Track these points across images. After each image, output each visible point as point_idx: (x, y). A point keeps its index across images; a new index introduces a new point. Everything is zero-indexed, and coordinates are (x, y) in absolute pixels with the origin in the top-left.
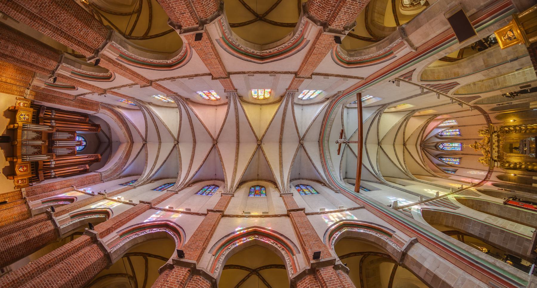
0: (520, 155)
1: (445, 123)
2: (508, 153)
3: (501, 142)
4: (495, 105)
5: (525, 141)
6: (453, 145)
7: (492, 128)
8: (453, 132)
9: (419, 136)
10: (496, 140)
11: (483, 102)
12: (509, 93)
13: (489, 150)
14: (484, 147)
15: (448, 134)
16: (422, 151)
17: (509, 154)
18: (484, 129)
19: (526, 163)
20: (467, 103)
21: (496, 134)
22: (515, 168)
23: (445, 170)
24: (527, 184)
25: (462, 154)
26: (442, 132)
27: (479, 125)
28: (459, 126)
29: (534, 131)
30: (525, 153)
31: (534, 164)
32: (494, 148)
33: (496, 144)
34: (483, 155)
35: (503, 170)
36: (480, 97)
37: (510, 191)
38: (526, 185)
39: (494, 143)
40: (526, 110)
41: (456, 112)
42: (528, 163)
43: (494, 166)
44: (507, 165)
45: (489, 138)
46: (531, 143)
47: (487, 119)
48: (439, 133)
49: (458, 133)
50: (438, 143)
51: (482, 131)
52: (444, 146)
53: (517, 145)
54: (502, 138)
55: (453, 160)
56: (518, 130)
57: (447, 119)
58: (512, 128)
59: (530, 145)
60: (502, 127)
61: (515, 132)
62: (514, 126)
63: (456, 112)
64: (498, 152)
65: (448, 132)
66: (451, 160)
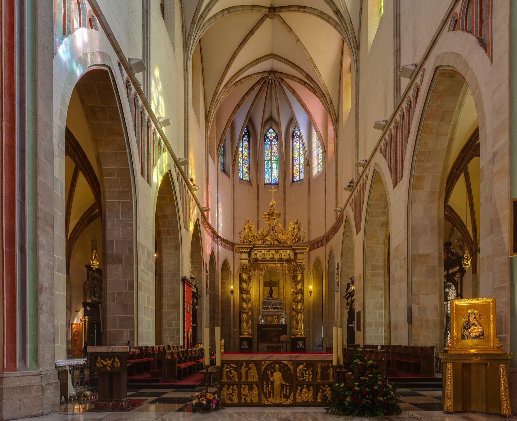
0: (261, 298)
1: (318, 147)
2: (264, 279)
3: (279, 265)
4: (338, 260)
5: (281, 308)
6: (275, 166)
7: (301, 249)
8: (300, 164)
9: (294, 65)
10: (283, 257)
11: (347, 237)
12: (354, 290)
13: (267, 243)
14: (272, 233)
16: (259, 77)
17: (262, 281)
18: (301, 234)
19: (250, 309)
20: (351, 201)
21: (292, 256)
22: (242, 290)
23: (224, 147)
24: (222, 312)
25: (258, 186)
26: (300, 137)
27: (309, 224)
28: (309, 178)
29: (294, 322)
30: (263, 308)
31: (250, 322)
32: (269, 251)
33: (277, 257)
34: (258, 230)
35: (237, 271)
36: (358, 233)
37: (207, 287)
38: (220, 312)
39: (277, 252)
40: (324, 315)
41: (337, 175)
42: (250, 313)
43: (241, 253)
44: (245, 276)
45: (285, 242)
46: (279, 317)
48: (299, 130)
49: (297, 178)
50: (278, 125)
51: (299, 229)
52: (271, 141)
53: (275, 295)
54: (286, 267)
55: (246, 166)
56: (296, 298)
57: (325, 151)
58: (299, 287)
59: (275, 315)
60: (302, 268)
61: (294, 292)
62: (303, 291)
63: (337, 175)
64: (264, 260)
65: (300, 154)
66: (246, 159)
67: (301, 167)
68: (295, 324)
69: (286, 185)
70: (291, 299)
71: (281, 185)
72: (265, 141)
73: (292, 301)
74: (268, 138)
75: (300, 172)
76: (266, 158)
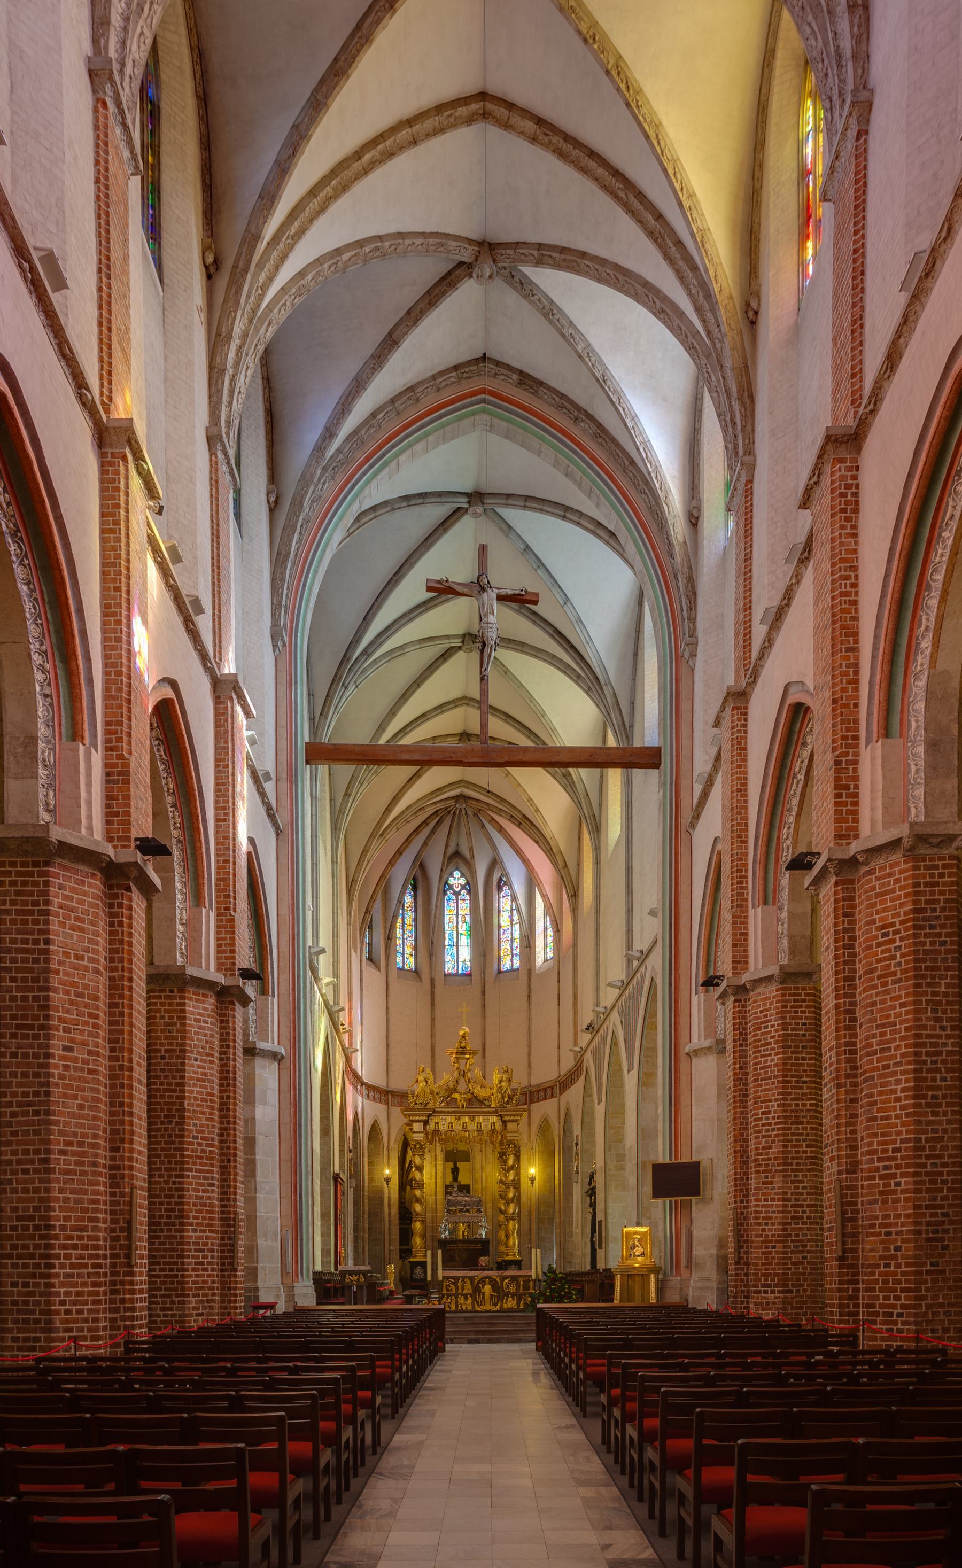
6: (464, 941)
8: (512, 940)
15: (505, 920)
24: (369, 1216)
27: (529, 1055)
35: (395, 1141)
47: (545, 1089)
49: (506, 964)
52: (457, 894)
55: (410, 942)
65: (512, 920)
66: (410, 930)
67: (515, 945)
68: (504, 1238)
69: (487, 979)
70: (497, 1194)
71: (476, 977)
72: (445, 893)
73: (497, 1197)
74: (451, 887)
75: (512, 955)
76: (447, 928)
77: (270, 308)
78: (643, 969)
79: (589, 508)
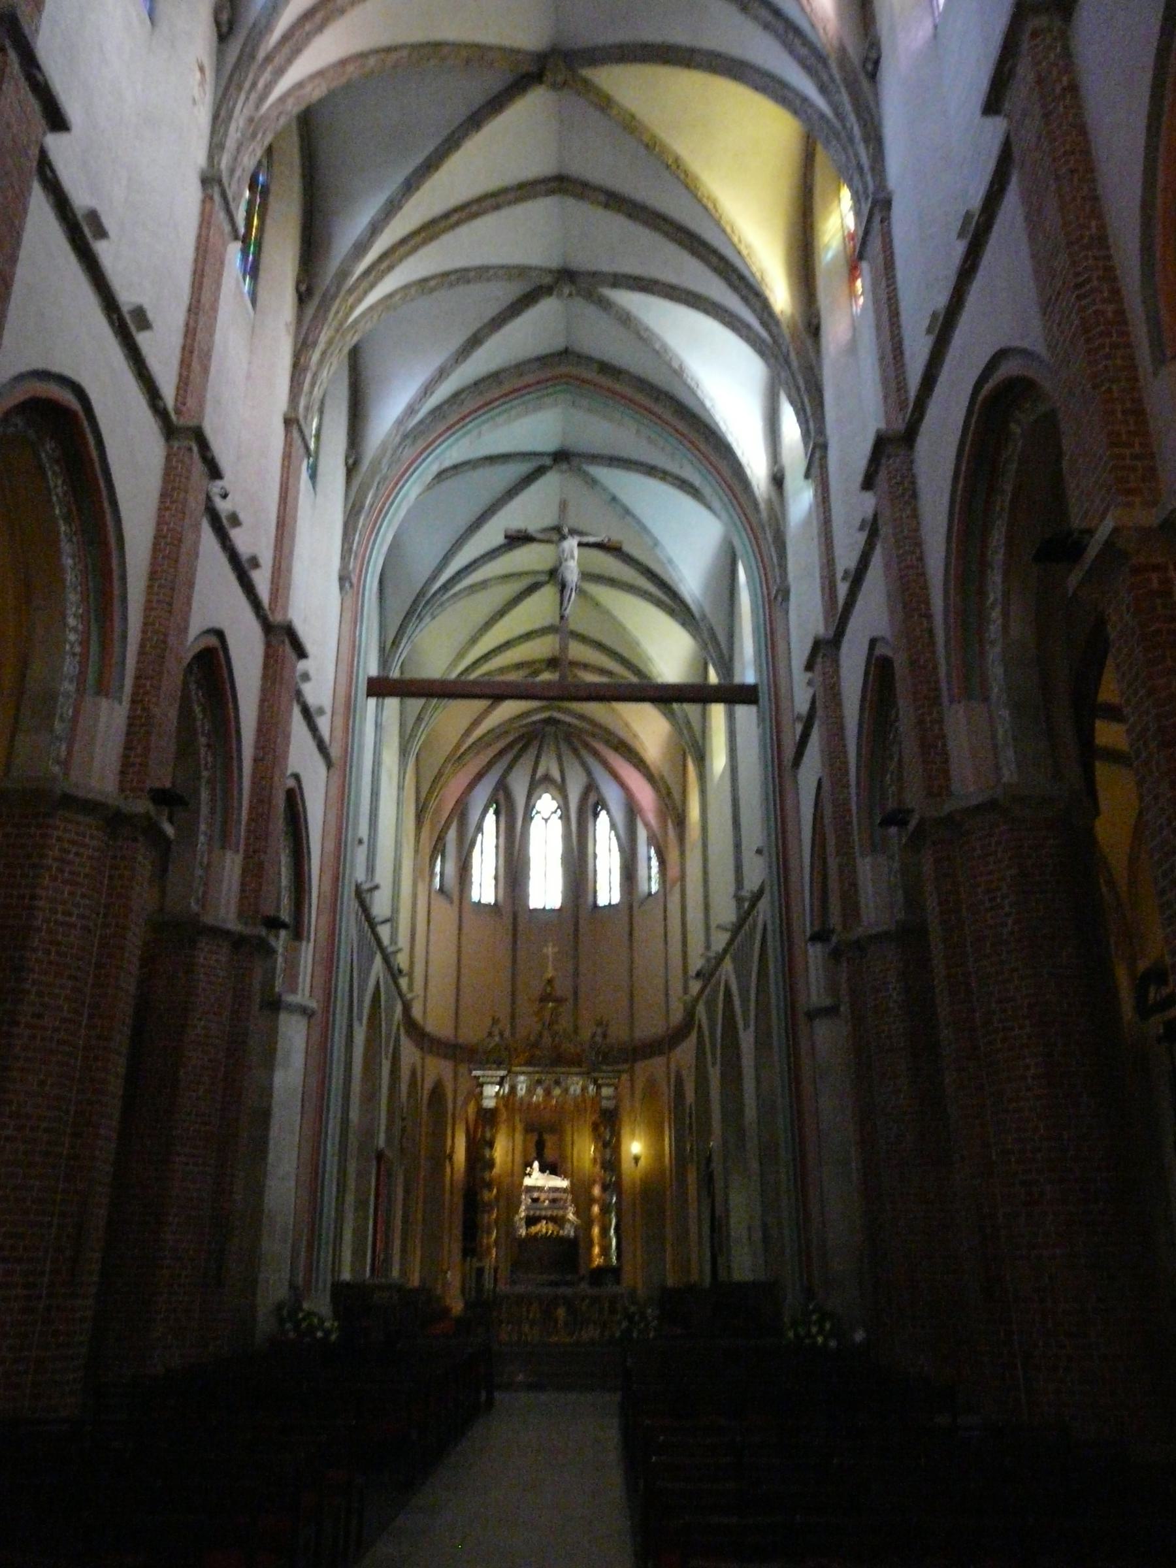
77: (356, 321)
78: (755, 912)
79: (673, 467)
